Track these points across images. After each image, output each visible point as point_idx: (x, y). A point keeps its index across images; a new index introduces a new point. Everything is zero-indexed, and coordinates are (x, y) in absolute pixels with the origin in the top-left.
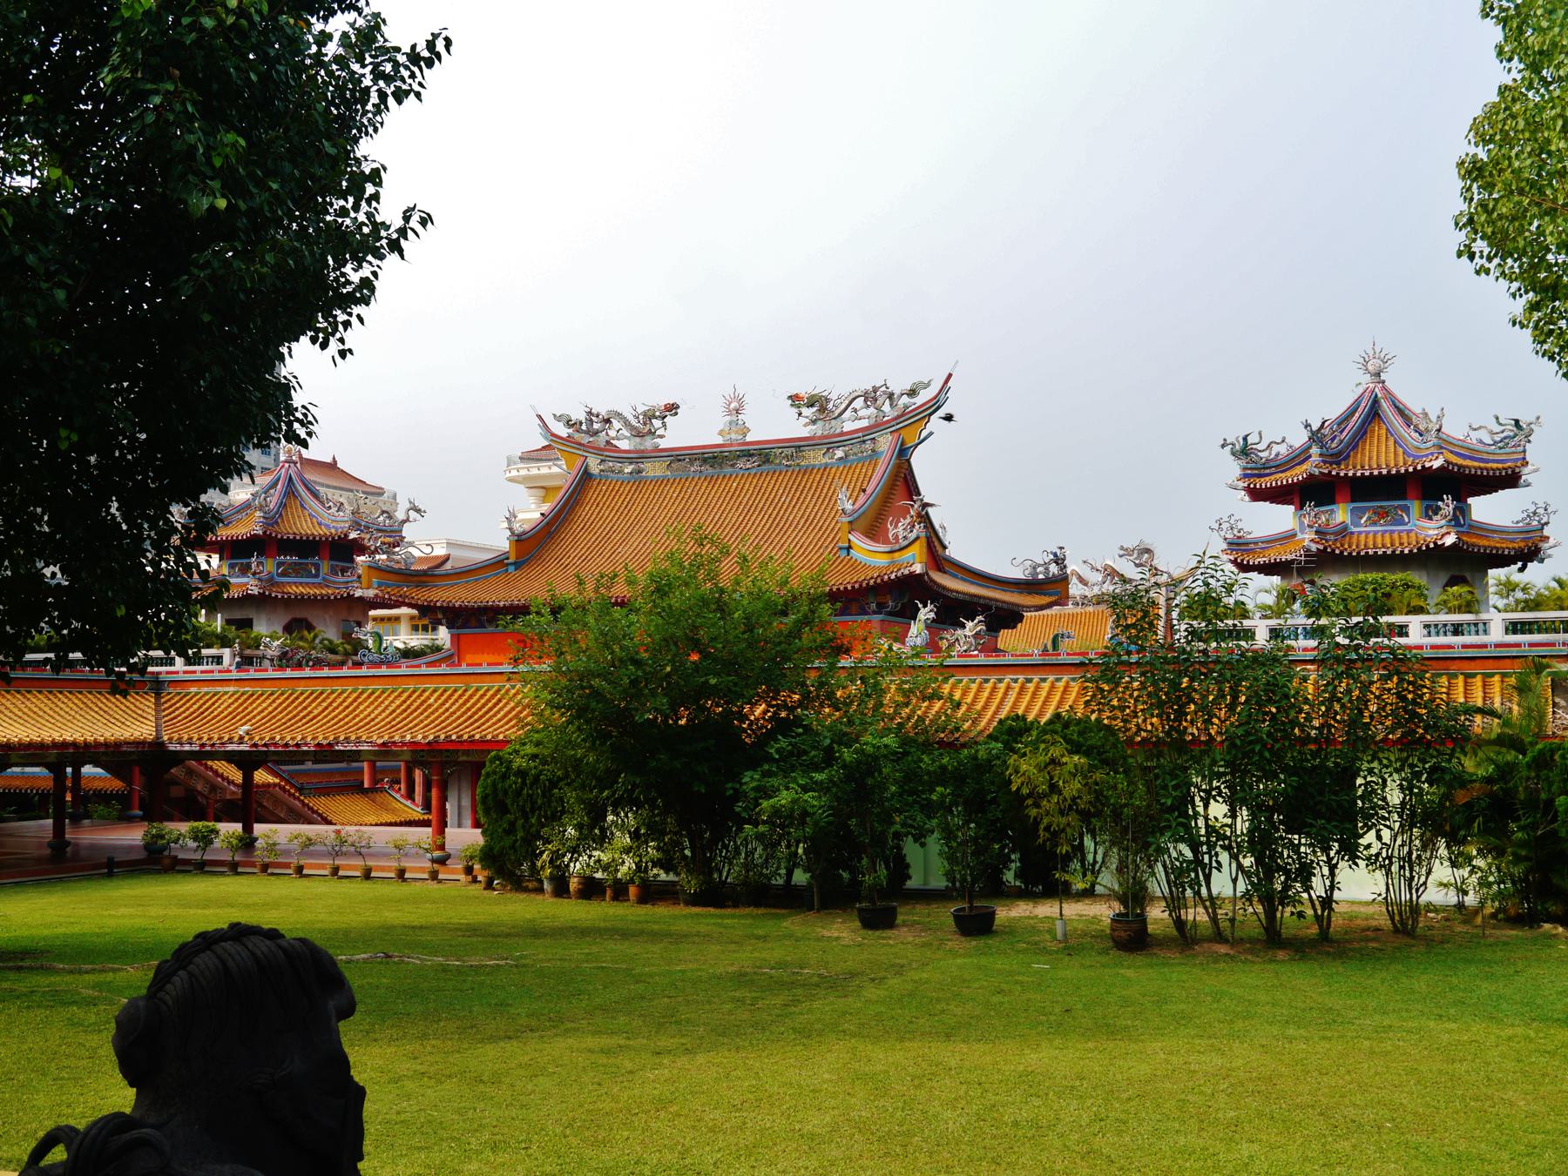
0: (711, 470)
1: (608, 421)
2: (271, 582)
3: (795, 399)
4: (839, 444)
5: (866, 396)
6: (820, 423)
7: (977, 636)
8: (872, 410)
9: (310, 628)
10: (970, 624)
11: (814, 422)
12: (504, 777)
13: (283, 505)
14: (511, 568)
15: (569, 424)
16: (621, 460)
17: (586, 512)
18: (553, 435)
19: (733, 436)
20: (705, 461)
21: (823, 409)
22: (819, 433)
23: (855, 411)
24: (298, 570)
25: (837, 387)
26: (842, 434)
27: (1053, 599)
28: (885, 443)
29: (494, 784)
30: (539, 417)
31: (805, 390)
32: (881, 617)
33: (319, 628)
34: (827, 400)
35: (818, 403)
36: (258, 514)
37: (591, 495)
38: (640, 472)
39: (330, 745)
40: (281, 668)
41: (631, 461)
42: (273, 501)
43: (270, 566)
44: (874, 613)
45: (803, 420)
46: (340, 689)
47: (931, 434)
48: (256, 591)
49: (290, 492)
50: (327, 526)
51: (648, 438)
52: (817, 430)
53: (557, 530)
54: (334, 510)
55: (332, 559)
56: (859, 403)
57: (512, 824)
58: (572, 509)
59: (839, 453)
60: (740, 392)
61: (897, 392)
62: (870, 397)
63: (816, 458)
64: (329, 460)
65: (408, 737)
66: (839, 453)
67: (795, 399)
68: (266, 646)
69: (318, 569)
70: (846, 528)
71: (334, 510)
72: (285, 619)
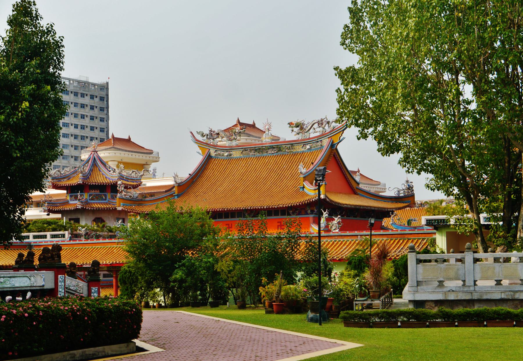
0: (258, 154)
1: (218, 134)
2: (87, 203)
3: (290, 124)
4: (308, 143)
5: (318, 122)
6: (301, 134)
7: (339, 223)
8: (321, 129)
9: (103, 221)
10: (336, 219)
11: (298, 134)
12: (125, 273)
13: (91, 170)
14: (176, 197)
15: (203, 135)
16: (223, 150)
17: (208, 172)
18: (197, 140)
19: (267, 140)
20: (256, 150)
21: (302, 128)
22: (300, 139)
23: (314, 129)
24: (98, 197)
25: (308, 119)
26: (309, 139)
27: (407, 204)
28: (326, 142)
29: (122, 276)
30: (191, 133)
31: (294, 121)
32: (312, 216)
33: (107, 221)
34: (303, 124)
35: (300, 126)
36: (80, 175)
37: (211, 165)
38: (231, 155)
39: (81, 265)
40: (87, 239)
41: (227, 151)
42: (87, 169)
43: (86, 196)
44: (311, 214)
45: (294, 133)
46: (87, 247)
47: (344, 138)
48: (80, 207)
49: (95, 164)
50: (109, 179)
51: (234, 141)
52: (300, 137)
53: (196, 181)
54: (112, 172)
55: (111, 192)
56: (316, 126)
57: (127, 287)
58: (203, 171)
59: (308, 147)
60: (270, 121)
61: (331, 121)
62: (320, 123)
63: (299, 149)
64: (127, 138)
65: (104, 263)
66: (308, 147)
67: (290, 124)
68: (80, 230)
69: (106, 197)
70: (302, 179)
71: (112, 172)
72: (93, 218)
